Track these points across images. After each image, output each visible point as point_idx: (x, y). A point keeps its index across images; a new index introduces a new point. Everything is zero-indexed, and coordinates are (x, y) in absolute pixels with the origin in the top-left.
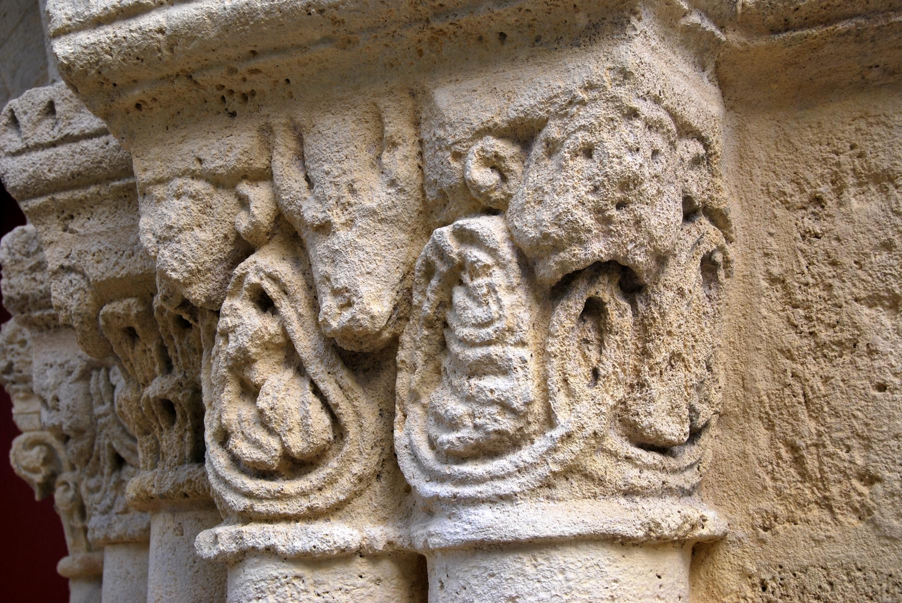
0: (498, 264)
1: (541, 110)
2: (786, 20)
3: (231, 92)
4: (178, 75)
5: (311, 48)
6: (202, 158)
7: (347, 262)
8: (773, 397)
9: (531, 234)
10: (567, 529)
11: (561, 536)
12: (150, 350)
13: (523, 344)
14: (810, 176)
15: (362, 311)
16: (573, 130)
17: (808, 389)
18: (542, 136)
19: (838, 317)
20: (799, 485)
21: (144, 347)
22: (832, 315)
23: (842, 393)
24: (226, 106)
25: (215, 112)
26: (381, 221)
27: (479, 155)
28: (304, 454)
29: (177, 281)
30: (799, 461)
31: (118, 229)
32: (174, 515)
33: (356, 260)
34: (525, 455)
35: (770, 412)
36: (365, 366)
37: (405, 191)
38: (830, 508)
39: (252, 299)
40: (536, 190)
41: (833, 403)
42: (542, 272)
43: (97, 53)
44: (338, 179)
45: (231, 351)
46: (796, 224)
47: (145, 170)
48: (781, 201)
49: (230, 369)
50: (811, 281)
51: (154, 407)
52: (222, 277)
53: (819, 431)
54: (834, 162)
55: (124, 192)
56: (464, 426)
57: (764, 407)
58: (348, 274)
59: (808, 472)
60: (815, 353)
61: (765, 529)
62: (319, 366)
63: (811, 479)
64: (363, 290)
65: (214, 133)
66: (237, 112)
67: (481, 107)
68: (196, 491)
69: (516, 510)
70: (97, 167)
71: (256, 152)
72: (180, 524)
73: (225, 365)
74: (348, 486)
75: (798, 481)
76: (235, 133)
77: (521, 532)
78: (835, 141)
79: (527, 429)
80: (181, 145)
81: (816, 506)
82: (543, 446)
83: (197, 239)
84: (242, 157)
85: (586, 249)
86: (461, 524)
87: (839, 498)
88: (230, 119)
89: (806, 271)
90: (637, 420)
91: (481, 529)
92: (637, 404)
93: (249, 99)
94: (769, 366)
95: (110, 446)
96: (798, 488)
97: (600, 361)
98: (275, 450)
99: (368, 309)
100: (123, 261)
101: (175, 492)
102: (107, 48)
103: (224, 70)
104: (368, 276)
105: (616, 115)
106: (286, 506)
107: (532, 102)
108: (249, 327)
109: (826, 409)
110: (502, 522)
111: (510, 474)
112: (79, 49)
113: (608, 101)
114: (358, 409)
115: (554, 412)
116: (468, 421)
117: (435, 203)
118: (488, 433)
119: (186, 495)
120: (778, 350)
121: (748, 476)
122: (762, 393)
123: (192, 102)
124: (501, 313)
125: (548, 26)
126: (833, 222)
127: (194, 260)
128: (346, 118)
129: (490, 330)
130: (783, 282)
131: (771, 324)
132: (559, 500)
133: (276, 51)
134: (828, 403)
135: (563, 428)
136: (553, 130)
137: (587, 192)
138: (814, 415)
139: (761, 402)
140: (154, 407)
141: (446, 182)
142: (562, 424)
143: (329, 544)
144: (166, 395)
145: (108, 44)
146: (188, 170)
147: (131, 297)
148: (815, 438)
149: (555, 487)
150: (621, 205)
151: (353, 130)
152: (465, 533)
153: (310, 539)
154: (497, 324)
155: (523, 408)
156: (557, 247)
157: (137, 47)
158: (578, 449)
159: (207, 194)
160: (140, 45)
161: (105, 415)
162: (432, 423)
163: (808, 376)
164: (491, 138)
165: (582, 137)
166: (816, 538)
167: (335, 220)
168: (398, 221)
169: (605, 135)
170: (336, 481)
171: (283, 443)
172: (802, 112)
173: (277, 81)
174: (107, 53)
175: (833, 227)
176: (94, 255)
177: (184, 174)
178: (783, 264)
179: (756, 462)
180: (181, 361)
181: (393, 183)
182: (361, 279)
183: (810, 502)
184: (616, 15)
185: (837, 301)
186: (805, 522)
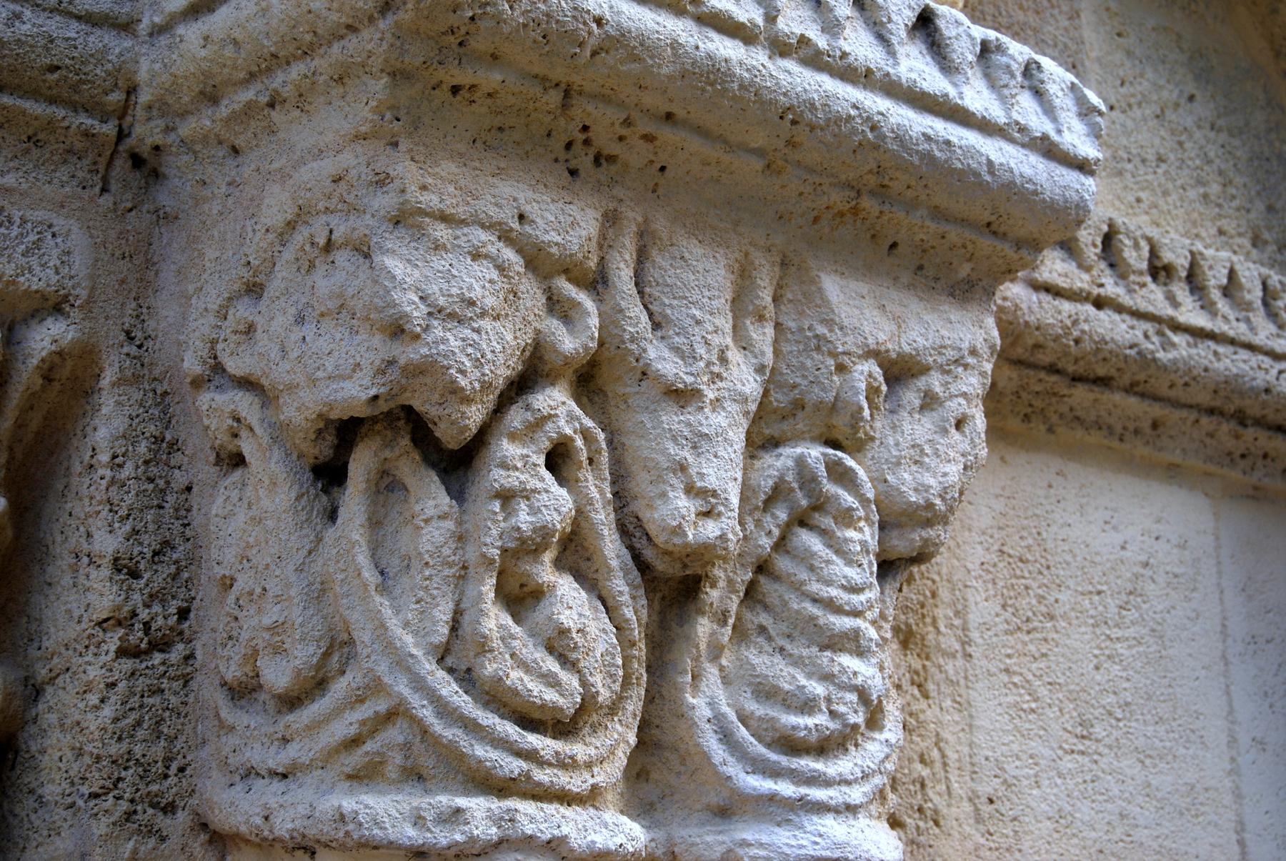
3: (587, 142)
7: (716, 456)
18: (921, 383)
45: (524, 527)
47: (424, 188)
56: (820, 710)
66: (582, 174)
73: (499, 544)
91: (838, 845)
111: (856, 780)
133: (701, 131)
136: (935, 382)
141: (816, 394)
146: (500, 224)
152: (816, 847)
153: (612, 833)
157: (558, 21)
160: (565, 22)
162: (749, 695)
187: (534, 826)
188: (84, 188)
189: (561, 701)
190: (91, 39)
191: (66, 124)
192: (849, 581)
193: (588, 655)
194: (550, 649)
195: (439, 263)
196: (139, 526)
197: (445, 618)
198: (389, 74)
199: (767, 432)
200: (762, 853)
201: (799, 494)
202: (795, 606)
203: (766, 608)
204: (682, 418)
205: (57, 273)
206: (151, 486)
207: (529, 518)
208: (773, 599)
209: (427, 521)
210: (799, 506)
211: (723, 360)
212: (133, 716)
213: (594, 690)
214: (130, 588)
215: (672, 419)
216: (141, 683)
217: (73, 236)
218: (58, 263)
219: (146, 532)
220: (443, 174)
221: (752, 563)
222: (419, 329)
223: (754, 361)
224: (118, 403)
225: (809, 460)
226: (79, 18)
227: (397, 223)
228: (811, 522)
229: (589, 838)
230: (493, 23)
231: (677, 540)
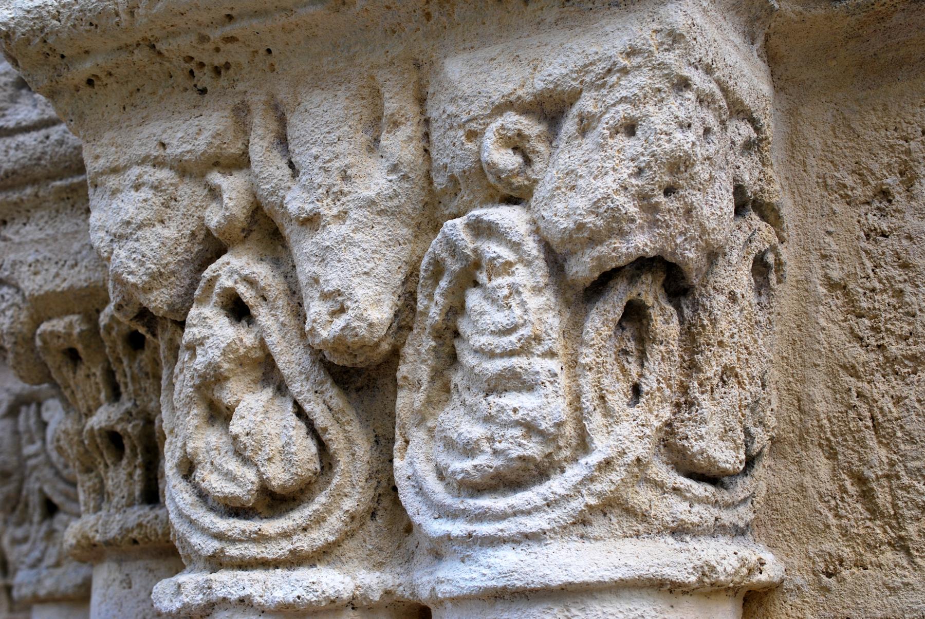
0: (521, 261)
1: (574, 80)
3: (202, 65)
4: (138, 45)
5: (298, 11)
6: (166, 142)
7: (339, 261)
8: (835, 421)
9: (562, 224)
10: (607, 573)
11: (599, 582)
12: (94, 374)
13: (551, 354)
14: (875, 167)
15: (359, 318)
16: (612, 102)
17: (876, 411)
18: (575, 110)
19: (911, 327)
20: (868, 523)
21: (87, 372)
22: (904, 325)
23: (918, 415)
24: (195, 82)
25: (181, 89)
26: (381, 212)
30: (867, 495)
31: (59, 236)
32: (120, 565)
33: (351, 259)
34: (556, 485)
35: (832, 438)
36: (359, 384)
37: (409, 177)
38: (907, 551)
39: (224, 307)
40: (567, 174)
41: (907, 427)
42: (574, 270)
43: (41, 18)
44: (329, 164)
45: (198, 367)
46: (859, 222)
47: (97, 157)
48: (840, 195)
49: (197, 388)
50: (878, 286)
51: (99, 440)
52: (188, 281)
53: (891, 460)
54: (904, 149)
55: (67, 193)
56: (482, 452)
57: (825, 433)
58: (341, 275)
59: (879, 507)
60: (884, 369)
61: (829, 575)
62: (304, 383)
63: (883, 515)
64: (359, 293)
66: (209, 89)
68: (147, 537)
69: (545, 551)
70: (36, 164)
71: (230, 135)
72: (127, 575)
75: (867, 518)
76: (205, 113)
77: (552, 577)
78: (904, 125)
79: (557, 455)
80: (141, 128)
81: (889, 548)
82: (577, 475)
83: (159, 236)
84: (214, 140)
85: (628, 241)
86: (478, 568)
87: (917, 538)
88: (199, 97)
89: (872, 275)
90: (686, 445)
91: (503, 575)
92: (685, 426)
93: (223, 72)
95: (41, 490)
96: (868, 527)
97: (641, 375)
98: (252, 483)
99: (365, 315)
100: (64, 272)
101: (123, 538)
102: (54, 12)
103: (194, 38)
104: (365, 277)
105: (664, 85)
106: (264, 550)
107: (564, 71)
109: (899, 434)
110: (529, 565)
111: (537, 509)
112: (21, 13)
113: (655, 68)
114: (350, 434)
116: (486, 446)
117: (444, 192)
118: (512, 460)
119: (135, 542)
120: (841, 366)
121: (807, 512)
122: (822, 416)
123: (154, 76)
124: (526, 317)
126: (903, 218)
128: (339, 93)
129: (513, 338)
130: (845, 287)
131: (830, 336)
132: (596, 539)
134: (902, 427)
135: (600, 454)
136: (587, 103)
137: (630, 175)
138: (885, 441)
139: (821, 427)
140: (99, 440)
142: (599, 448)
143: (316, 594)
144: (113, 426)
145: (56, 7)
147: (74, 313)
148: (887, 468)
149: (591, 525)
150: (669, 191)
151: (346, 108)
152: (483, 579)
155: (552, 430)
156: (594, 239)
157: (90, 10)
158: (619, 478)
159: (171, 184)
161: (36, 455)
162: (441, 449)
163: (876, 396)
164: (514, 113)
165: (623, 110)
166: (891, 585)
167: (324, 211)
168: (400, 212)
169: (651, 108)
171: (260, 474)
172: (865, 93)
173: (257, 52)
174: (54, 17)
175: (903, 224)
176: (30, 266)
177: (143, 161)
178: (845, 267)
179: (816, 496)
180: (131, 387)
181: (394, 168)
182: (357, 280)
183: (882, 543)
185: (910, 309)
186: (877, 566)
193: (260, 450)
220: (106, 141)
230: (54, 37)
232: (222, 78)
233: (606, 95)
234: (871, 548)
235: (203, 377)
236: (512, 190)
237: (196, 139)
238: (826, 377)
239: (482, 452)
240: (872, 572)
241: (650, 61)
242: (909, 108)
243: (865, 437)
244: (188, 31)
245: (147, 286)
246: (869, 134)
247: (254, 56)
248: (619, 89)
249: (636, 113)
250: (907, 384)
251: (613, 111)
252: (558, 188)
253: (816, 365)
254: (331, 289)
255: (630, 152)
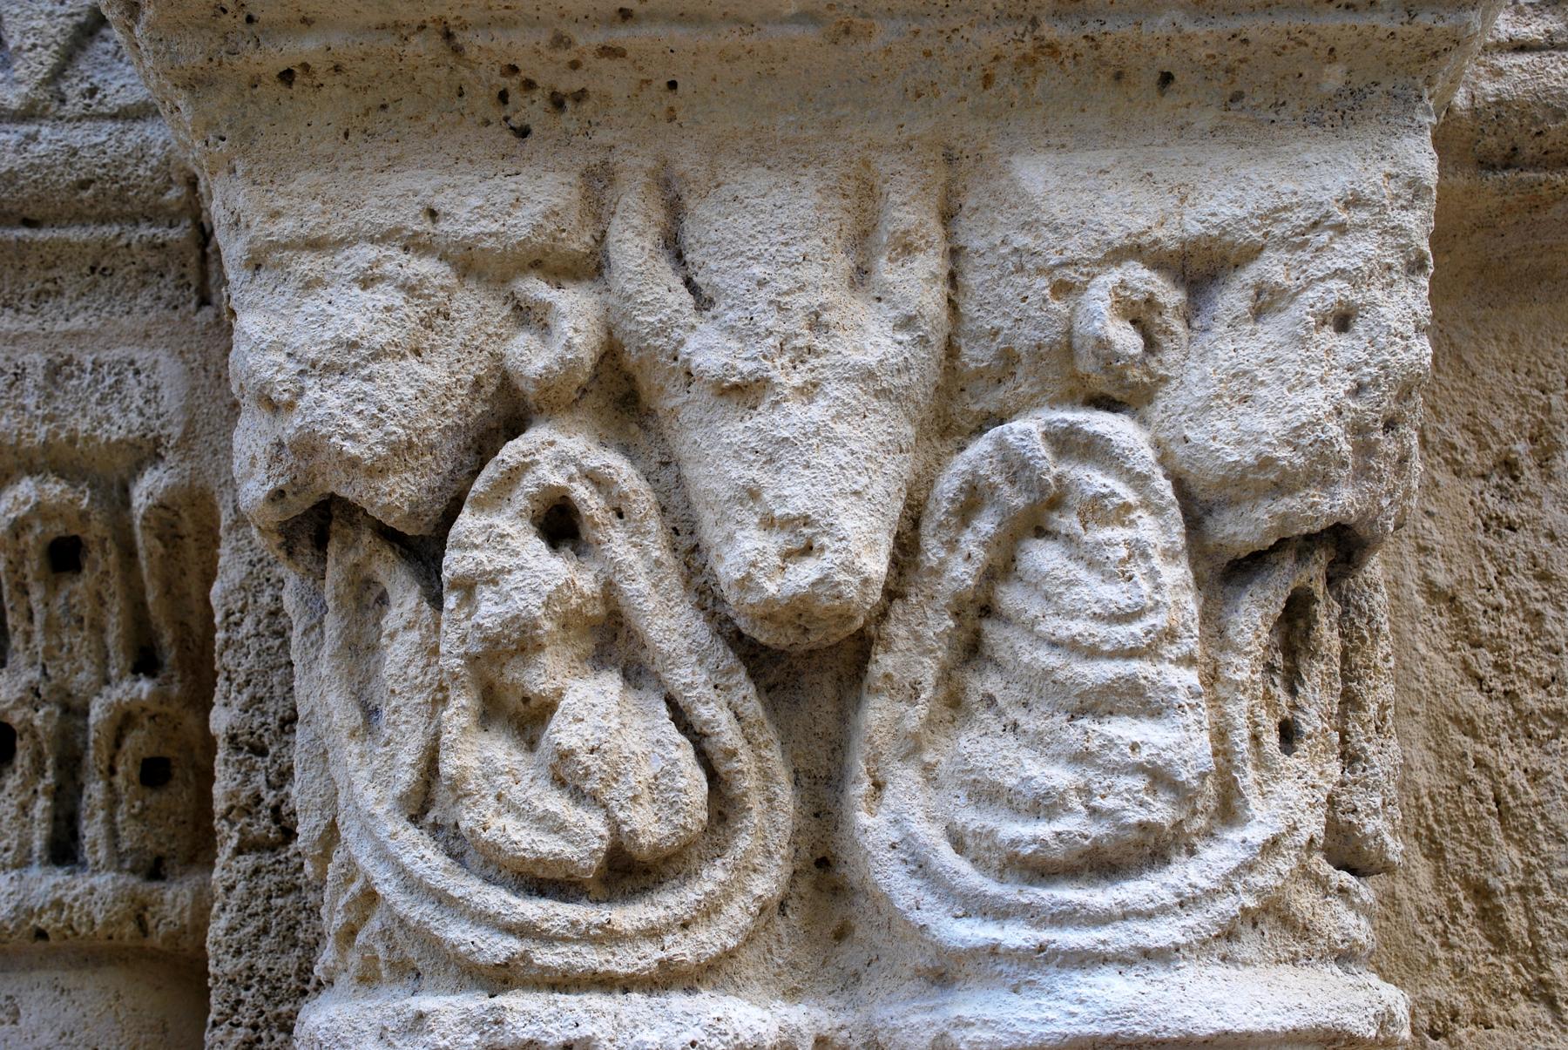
0: (1146, 504)
1: (1254, 228)
2: (1514, 149)
3: (529, 85)
4: (422, 27)
5: (768, 28)
7: (807, 466)
10: (1277, 1019)
11: (1267, 1032)
13: (1189, 661)
14: (1498, 424)
15: (848, 568)
16: (1320, 274)
17: (1505, 790)
18: (1249, 275)
19: (1554, 670)
20: (1491, 959)
22: (1543, 664)
24: (508, 111)
25: (479, 120)
27: (1117, 294)
28: (661, 850)
29: (354, 462)
30: (1490, 916)
34: (1185, 874)
35: (1435, 826)
36: (771, 680)
37: (928, 341)
38: (1551, 1003)
39: (533, 521)
40: (1234, 376)
41: (1553, 817)
44: (788, 299)
45: (487, 623)
46: (1472, 503)
47: (275, 215)
48: (1445, 460)
49: (472, 660)
50: (1506, 603)
52: (450, 466)
53: (1529, 864)
54: (1541, 403)
56: (1070, 811)
57: (1426, 817)
58: (813, 490)
59: (1509, 935)
60: (1513, 728)
62: (697, 669)
63: (1515, 949)
64: (847, 524)
65: (471, 161)
66: (535, 129)
67: (1124, 205)
68: (71, 928)
69: (1177, 979)
71: (574, 216)
72: (8, 998)
73: (462, 650)
74: (745, 921)
75: (1489, 950)
77: (1198, 1021)
78: (1542, 369)
80: (385, 176)
82: (1227, 858)
83: (414, 378)
84: (545, 223)
85: (1333, 495)
86: (1057, 1004)
88: (515, 141)
89: (1495, 585)
90: (1356, 822)
92: (1349, 792)
93: (569, 104)
94: (1432, 744)
96: (1491, 964)
97: (1295, 707)
98: (601, 837)
99: (858, 564)
101: (18, 927)
103: (545, 38)
104: (853, 498)
105: (1396, 260)
106: (610, 957)
107: (1240, 213)
108: (543, 576)
109: (1540, 827)
110: (1156, 1001)
111: (1164, 910)
113: (1386, 232)
114: (770, 764)
115: (1242, 796)
116: (1075, 803)
117: (979, 374)
119: (41, 934)
120: (1450, 718)
121: (1402, 938)
122: (1424, 791)
123: (428, 89)
124: (1158, 597)
125: (1266, 77)
126: (1539, 506)
127: (405, 422)
128: (803, 179)
129: (1137, 628)
130: (1453, 599)
132: (1245, 964)
134: (1543, 817)
135: (1262, 827)
136: (1273, 268)
137: (1347, 392)
138: (1516, 836)
139: (1421, 808)
143: (725, 1039)
146: (398, 230)
148: (1522, 877)
149: (1238, 940)
151: (819, 207)
152: (1072, 1021)
153: (679, 1028)
154: (1149, 620)
155: (1195, 783)
156: (1283, 485)
158: (1288, 868)
159: (442, 288)
162: (963, 800)
163: (1505, 768)
167: (777, 376)
169: (1379, 294)
170: (717, 910)
171: (615, 826)
173: (648, 82)
175: (1540, 515)
177: (385, 237)
178: (1454, 568)
180: (38, 639)
181: (907, 323)
182: (842, 503)
183: (1513, 989)
184: (1401, 81)
185: (1552, 642)
186: (1507, 1023)
187: (534, 1028)
188: (176, 307)
189: (569, 851)
190: (131, 135)
191: (123, 241)
192: (1105, 607)
193: (616, 780)
194: (560, 782)
195: (310, 305)
196: (261, 692)
197: (409, 760)
198: (184, 87)
199: (977, 408)
200: (987, 1035)
201: (1006, 490)
202: (1026, 658)
203: (999, 666)
204: (749, 424)
205: (141, 413)
206: (278, 642)
207: (496, 610)
208: (1002, 654)
209: (392, 636)
210: (1016, 508)
211: (816, 323)
212: (258, 922)
213: (627, 829)
214: (253, 768)
215: (736, 429)
216: (267, 882)
217: (161, 368)
218: (141, 403)
219: (272, 698)
220: (301, 189)
221: (947, 606)
222: (286, 396)
223: (893, 313)
224: (236, 550)
225: (1011, 438)
226: (114, 117)
227: (258, 267)
228: (1050, 528)
229: (637, 1038)
231: (752, 598)
232: (567, 115)
233: (1307, 262)
234: (1500, 996)
235: (493, 642)
236: (1122, 388)
237: (509, 215)
238: (1426, 734)
239: (1070, 811)
240: (1502, 1034)
241: (1380, 221)
242: (1548, 343)
243: (1489, 828)
244: (535, 22)
245: (380, 465)
246: (1489, 374)
247: (641, 89)
248: (1330, 255)
249: (1357, 298)
250: (1548, 754)
251: (1320, 288)
252: (1219, 396)
253: (1414, 713)
254: (794, 513)
255: (1345, 357)
